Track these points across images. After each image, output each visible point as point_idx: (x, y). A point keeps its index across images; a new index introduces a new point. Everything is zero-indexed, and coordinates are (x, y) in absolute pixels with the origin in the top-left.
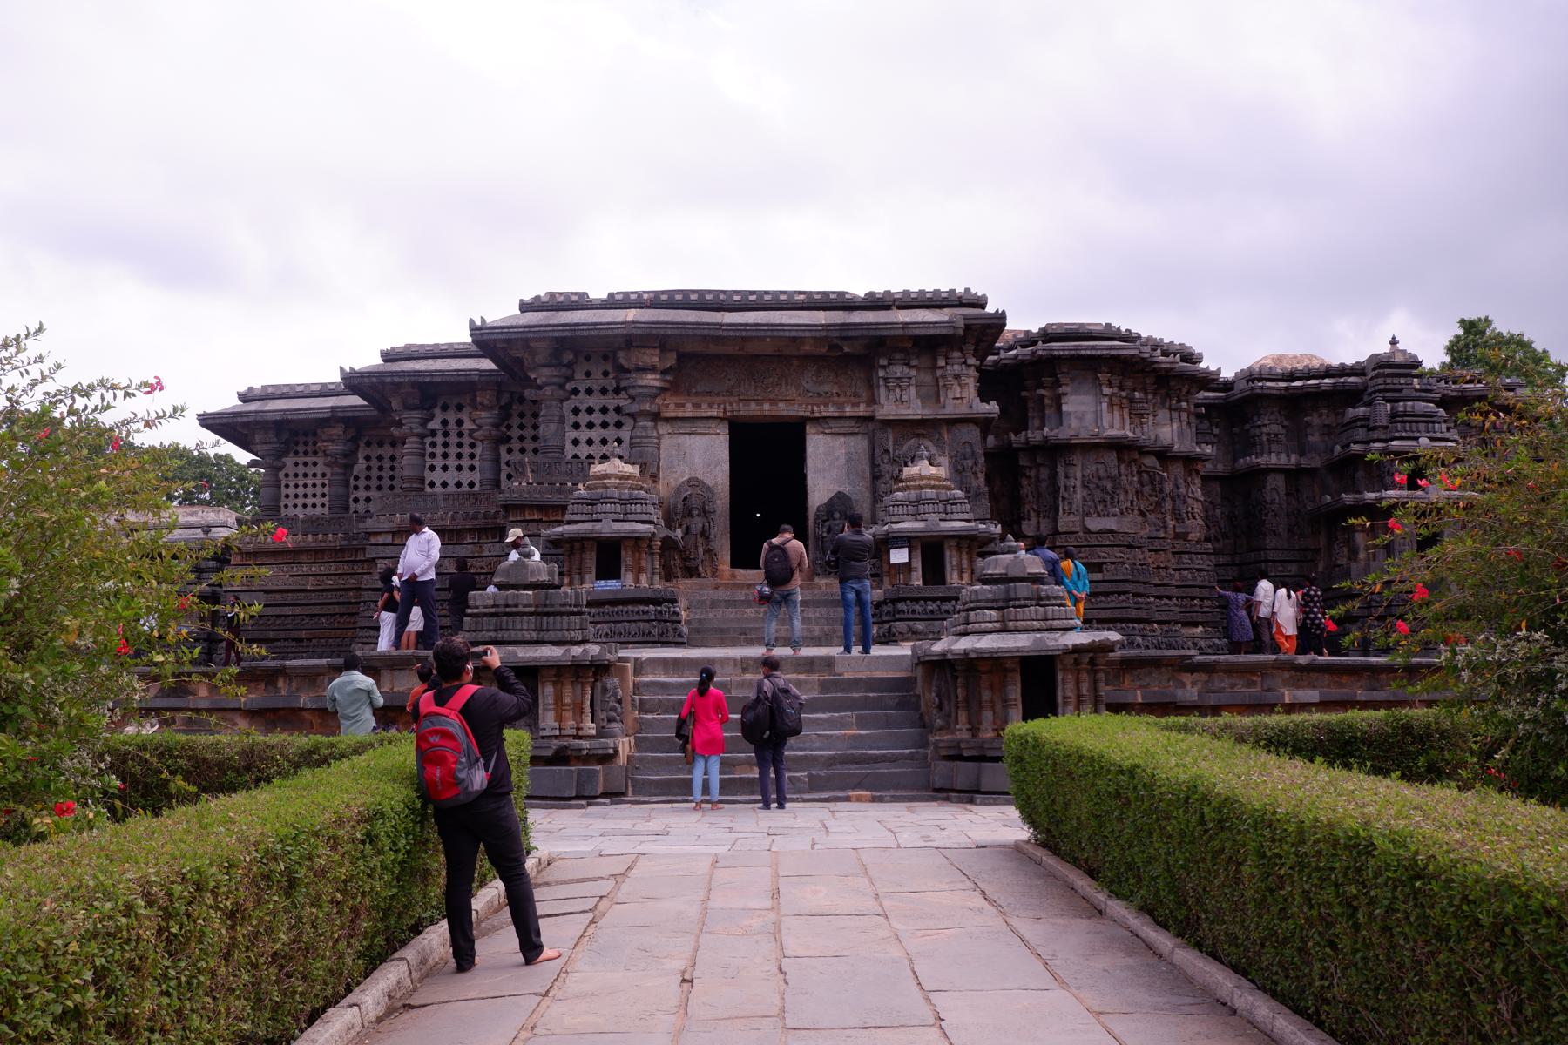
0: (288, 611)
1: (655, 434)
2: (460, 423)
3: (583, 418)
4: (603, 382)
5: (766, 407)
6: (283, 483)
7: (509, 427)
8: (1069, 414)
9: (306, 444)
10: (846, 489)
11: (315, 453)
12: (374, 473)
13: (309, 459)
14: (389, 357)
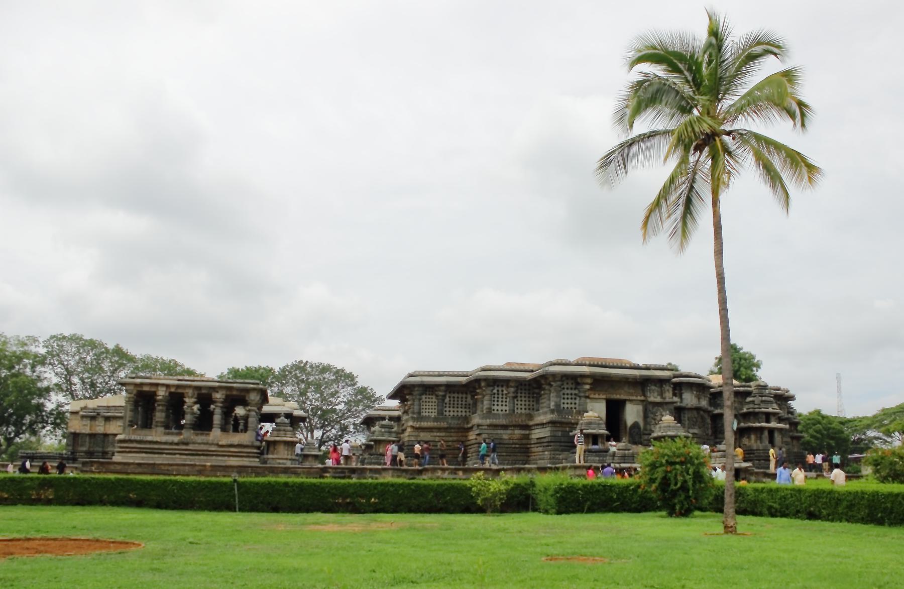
2: (502, 391)
7: (517, 393)
10: (637, 420)
11: (432, 395)
12: (452, 402)
13: (430, 397)
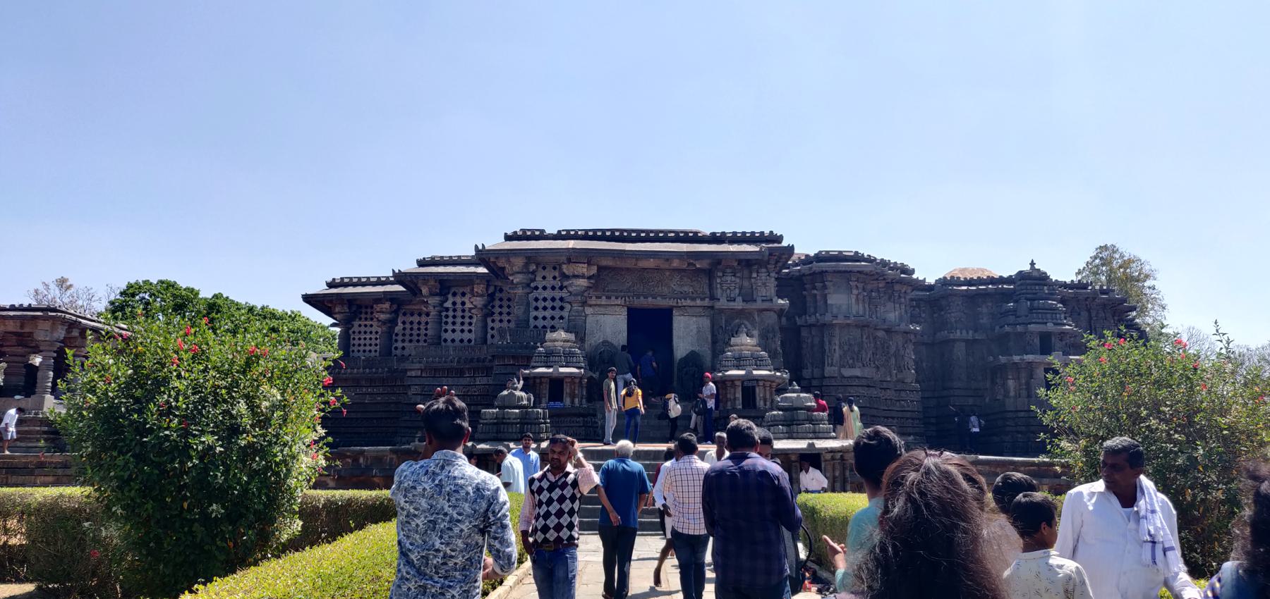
1: (583, 314)
2: (463, 304)
3: (541, 304)
4: (553, 283)
5: (650, 299)
6: (352, 337)
7: (493, 307)
8: (832, 305)
9: (366, 313)
10: (696, 349)
11: (372, 319)
13: (369, 323)
14: (421, 263)
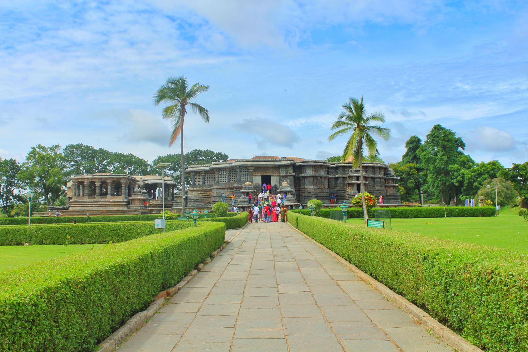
0: (198, 199)
2: (224, 173)
3: (243, 175)
4: (245, 170)
10: (276, 184)
12: (208, 178)
